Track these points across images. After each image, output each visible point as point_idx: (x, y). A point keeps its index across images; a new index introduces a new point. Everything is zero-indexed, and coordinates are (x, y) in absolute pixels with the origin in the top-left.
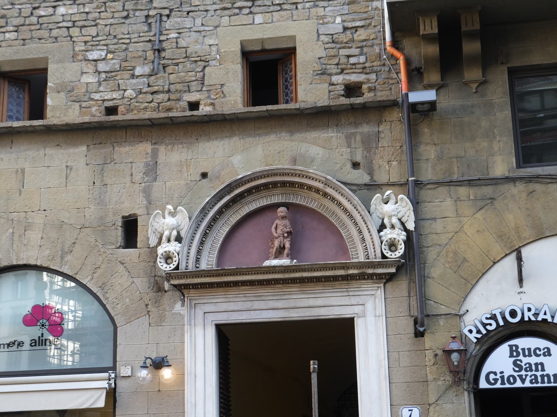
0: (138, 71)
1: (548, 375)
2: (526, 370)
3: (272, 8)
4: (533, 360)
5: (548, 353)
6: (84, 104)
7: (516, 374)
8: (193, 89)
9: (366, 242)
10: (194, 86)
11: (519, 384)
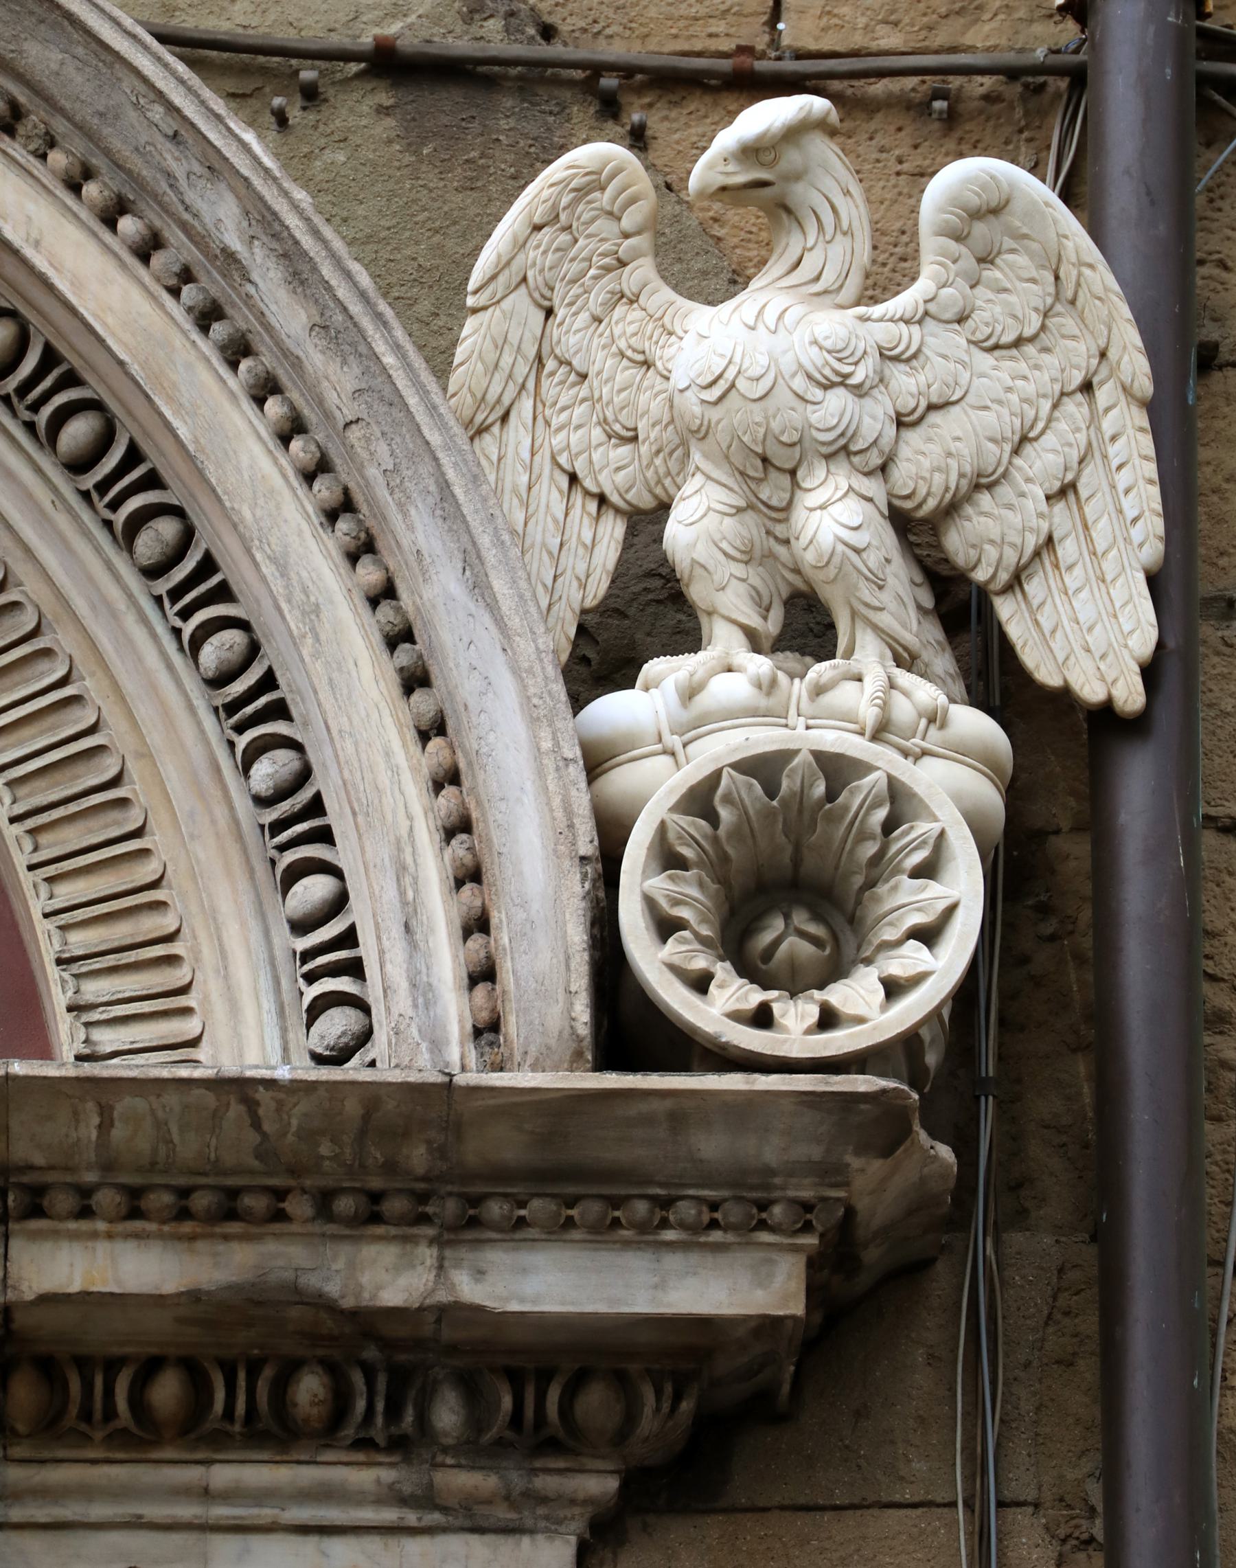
9: (343, 854)
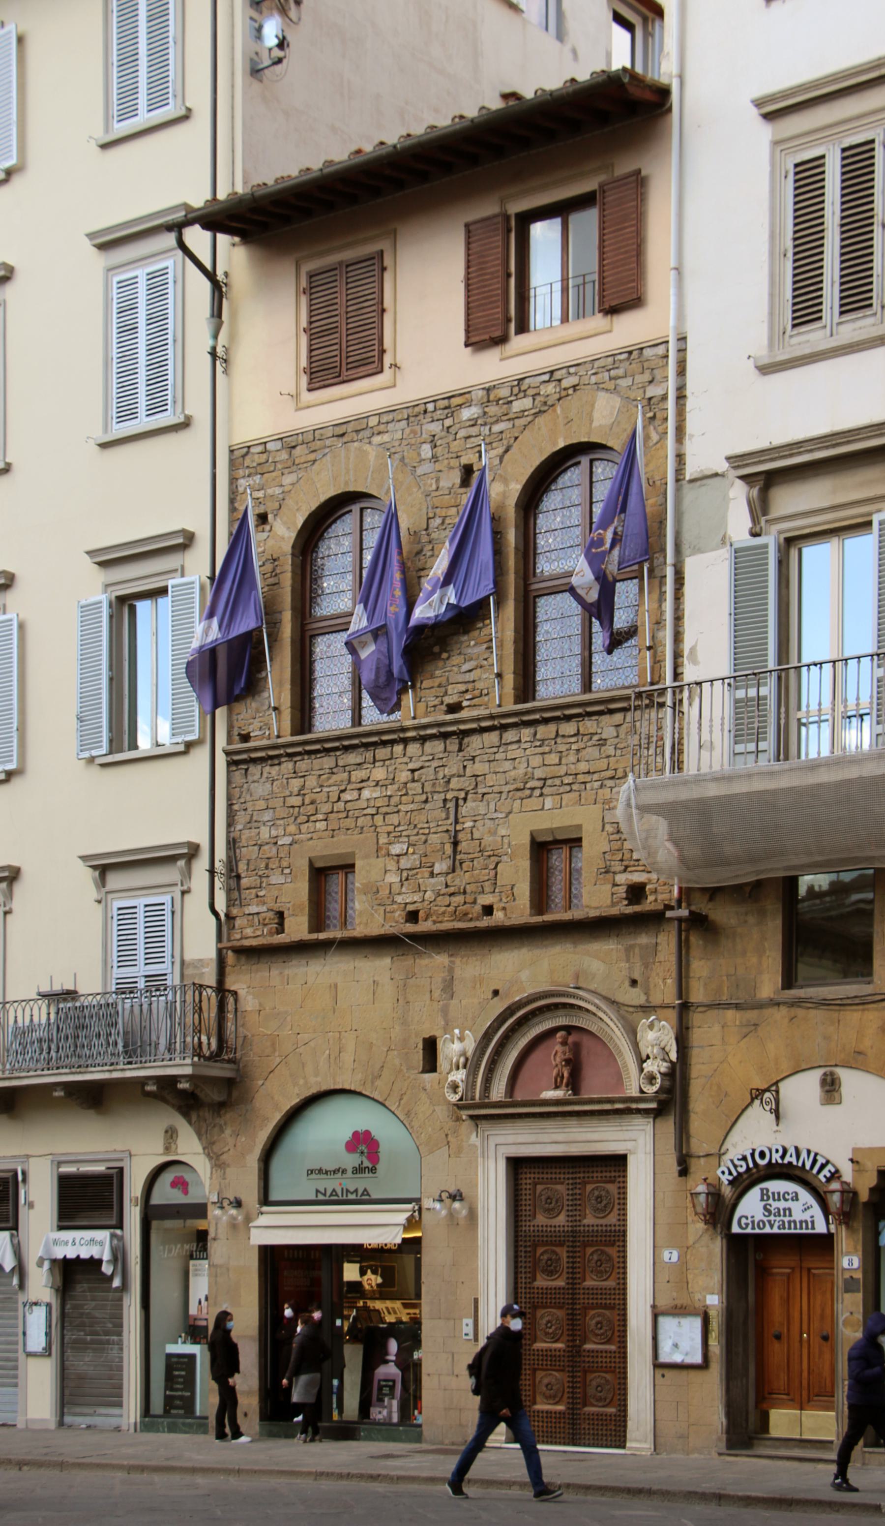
0: (437, 869)
1: (795, 1222)
2: (775, 1216)
3: (562, 790)
4: (782, 1204)
5: (796, 1198)
6: (388, 908)
7: (765, 1219)
8: (487, 889)
10: (488, 887)
11: (767, 1230)
